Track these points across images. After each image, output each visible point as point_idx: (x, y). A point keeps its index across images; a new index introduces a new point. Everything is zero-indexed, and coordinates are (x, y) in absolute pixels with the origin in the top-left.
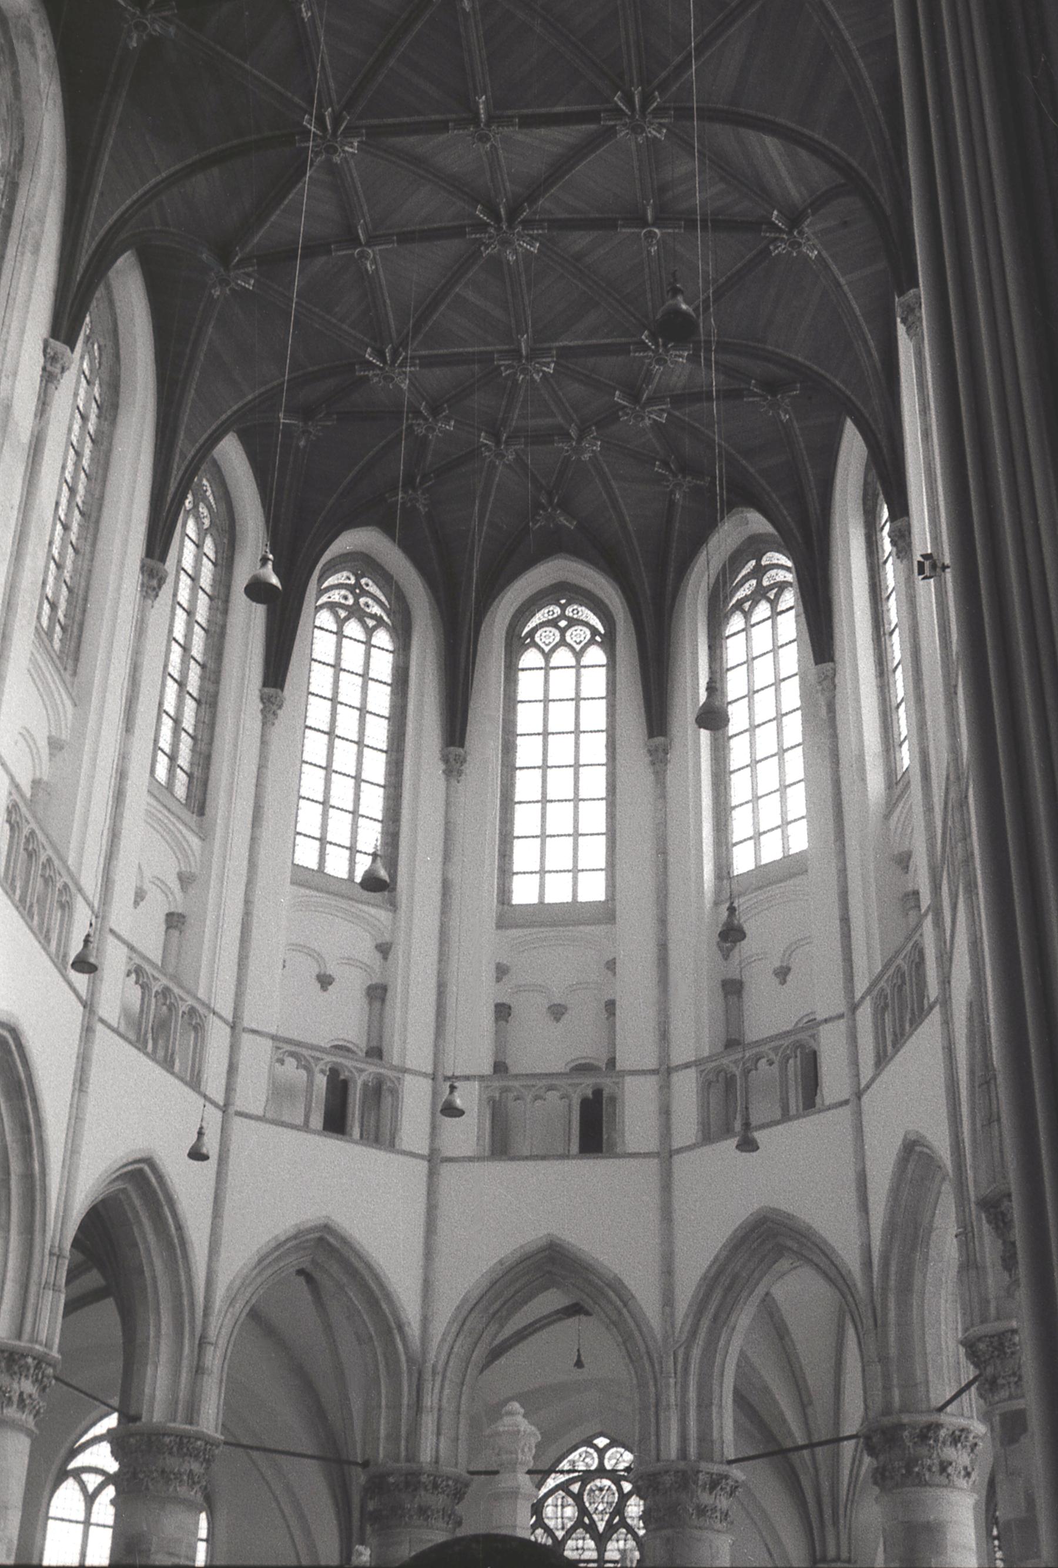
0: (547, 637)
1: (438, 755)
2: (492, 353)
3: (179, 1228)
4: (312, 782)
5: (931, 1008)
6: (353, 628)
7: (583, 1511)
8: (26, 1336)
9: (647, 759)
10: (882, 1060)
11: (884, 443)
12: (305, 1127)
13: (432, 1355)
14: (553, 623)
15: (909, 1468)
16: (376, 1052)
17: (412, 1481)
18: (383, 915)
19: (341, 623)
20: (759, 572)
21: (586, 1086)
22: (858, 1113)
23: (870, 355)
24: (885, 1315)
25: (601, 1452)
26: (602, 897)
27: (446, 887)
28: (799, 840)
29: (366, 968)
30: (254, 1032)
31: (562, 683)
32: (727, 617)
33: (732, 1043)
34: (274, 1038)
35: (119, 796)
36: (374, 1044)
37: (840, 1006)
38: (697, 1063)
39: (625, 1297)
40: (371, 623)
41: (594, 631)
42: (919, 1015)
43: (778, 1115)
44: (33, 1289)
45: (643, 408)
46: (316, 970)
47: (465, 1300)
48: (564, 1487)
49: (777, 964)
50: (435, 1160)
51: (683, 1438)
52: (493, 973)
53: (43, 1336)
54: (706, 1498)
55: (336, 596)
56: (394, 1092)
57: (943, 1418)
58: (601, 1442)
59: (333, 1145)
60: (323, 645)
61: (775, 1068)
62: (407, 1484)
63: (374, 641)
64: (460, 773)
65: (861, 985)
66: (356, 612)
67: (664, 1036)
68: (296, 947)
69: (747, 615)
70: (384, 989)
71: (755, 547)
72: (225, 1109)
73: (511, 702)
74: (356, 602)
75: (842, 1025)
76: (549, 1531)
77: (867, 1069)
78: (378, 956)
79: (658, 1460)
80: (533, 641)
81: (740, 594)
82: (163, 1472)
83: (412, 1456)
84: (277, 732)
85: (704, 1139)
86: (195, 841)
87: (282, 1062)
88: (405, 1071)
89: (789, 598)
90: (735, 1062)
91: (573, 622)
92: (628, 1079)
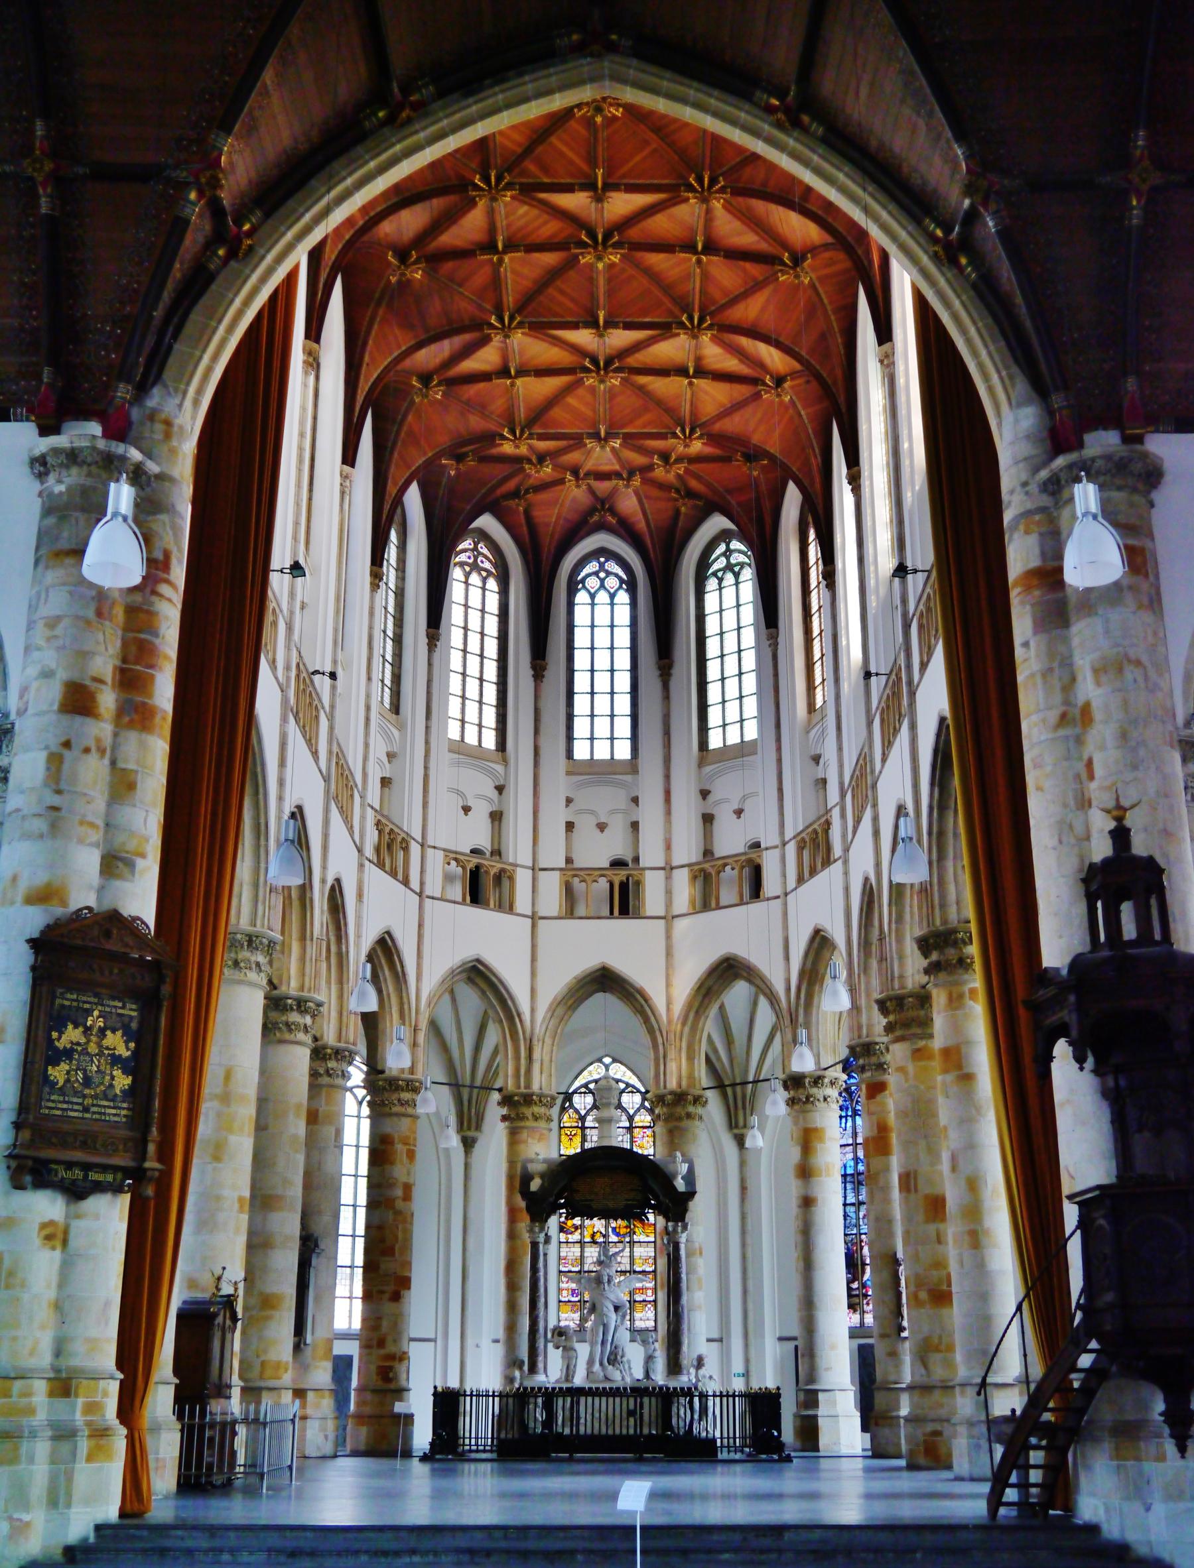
0: (593, 583)
1: (529, 665)
2: (582, 434)
3: (402, 966)
4: (455, 682)
5: (835, 861)
6: (475, 579)
8: (343, 1039)
9: (657, 673)
10: (801, 880)
11: (821, 512)
12: (463, 902)
13: (537, 1031)
14: (596, 574)
15: (808, 1098)
16: (497, 852)
17: (528, 1099)
18: (499, 768)
19: (467, 575)
20: (728, 553)
21: (619, 876)
22: (785, 904)
23: (815, 457)
24: (797, 1016)
25: (607, 1067)
26: (628, 757)
28: (752, 732)
29: (490, 801)
30: (434, 847)
32: (706, 578)
33: (708, 853)
34: (444, 850)
35: (367, 719)
36: (496, 847)
37: (776, 841)
38: (689, 865)
40: (484, 574)
42: (827, 862)
43: (736, 900)
44: (345, 1014)
45: (671, 465)
46: (461, 804)
47: (555, 999)
48: (586, 1086)
49: (736, 807)
50: (534, 918)
52: (564, 802)
53: (351, 1040)
54: (691, 1109)
55: (463, 557)
56: (511, 879)
57: (827, 1073)
60: (456, 591)
61: (736, 872)
62: (525, 1100)
63: (487, 586)
64: (543, 676)
65: (789, 834)
66: (475, 567)
67: (668, 847)
68: (451, 790)
70: (501, 814)
71: (724, 536)
72: (420, 895)
74: (476, 560)
75: (777, 852)
76: (577, 1111)
77: (792, 882)
78: (496, 792)
79: (665, 1087)
80: (584, 587)
81: (715, 567)
82: (399, 1100)
83: (528, 1086)
84: (436, 655)
86: (396, 732)
87: (449, 864)
88: (516, 865)
89: (748, 574)
90: (713, 867)
92: (647, 872)
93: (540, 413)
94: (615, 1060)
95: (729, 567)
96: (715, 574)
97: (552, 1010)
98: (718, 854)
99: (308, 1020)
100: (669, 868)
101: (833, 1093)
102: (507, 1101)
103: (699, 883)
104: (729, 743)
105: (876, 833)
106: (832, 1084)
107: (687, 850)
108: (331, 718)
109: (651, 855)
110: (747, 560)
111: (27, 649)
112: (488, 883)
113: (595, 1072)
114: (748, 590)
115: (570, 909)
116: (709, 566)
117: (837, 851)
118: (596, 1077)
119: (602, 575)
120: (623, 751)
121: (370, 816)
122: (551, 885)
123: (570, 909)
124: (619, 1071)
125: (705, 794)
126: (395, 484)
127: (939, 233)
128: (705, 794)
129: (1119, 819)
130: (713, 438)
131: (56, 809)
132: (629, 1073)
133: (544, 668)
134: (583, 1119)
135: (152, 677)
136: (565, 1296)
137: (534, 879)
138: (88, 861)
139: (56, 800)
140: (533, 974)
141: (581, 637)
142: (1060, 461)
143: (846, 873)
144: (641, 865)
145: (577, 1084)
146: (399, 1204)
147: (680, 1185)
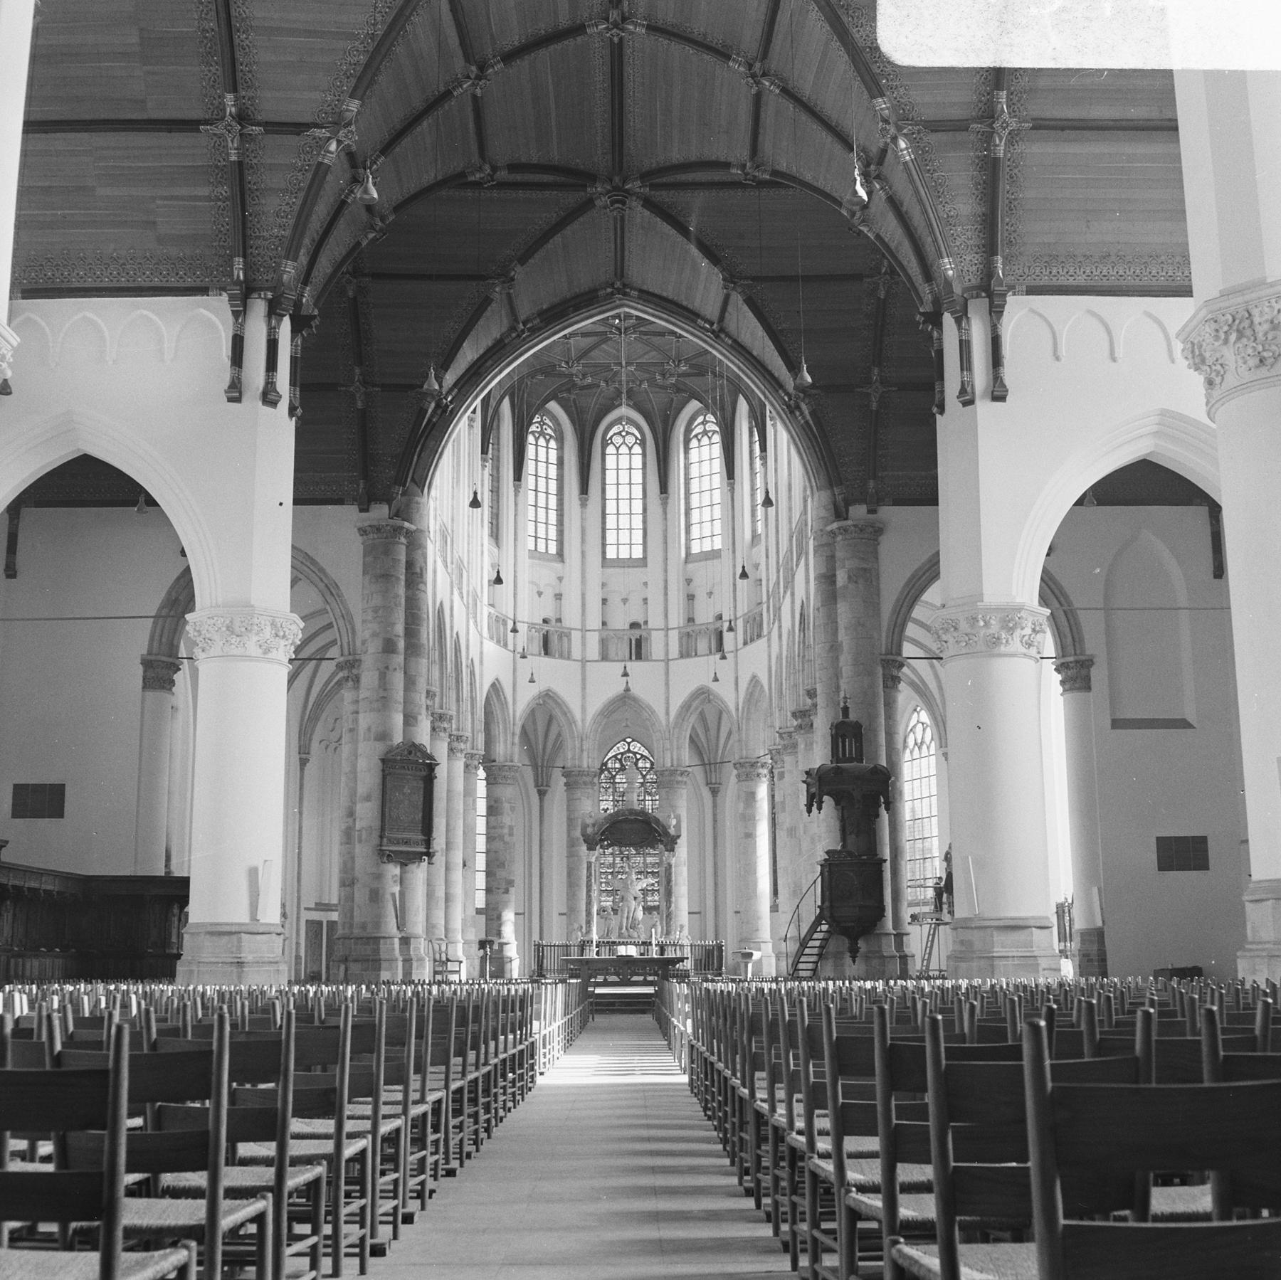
6: (542, 442)
7: (622, 765)
10: (745, 643)
12: (540, 654)
14: (619, 433)
16: (559, 620)
17: (581, 773)
18: (558, 566)
19: (537, 439)
20: (704, 423)
21: (636, 633)
22: (736, 657)
25: (629, 744)
27: (583, 554)
31: (624, 461)
32: (691, 440)
33: (691, 620)
38: (679, 628)
39: (653, 712)
41: (637, 438)
42: (759, 636)
46: (536, 590)
48: (615, 756)
50: (584, 662)
51: (672, 760)
54: (680, 778)
58: (629, 740)
59: (546, 660)
60: (530, 451)
65: (739, 614)
66: (542, 434)
67: (666, 616)
69: (699, 440)
70: (561, 595)
73: (604, 470)
85: (681, 652)
86: (496, 550)
89: (717, 438)
91: (628, 433)
92: (653, 632)
93: (585, 353)
94: (633, 741)
95: (705, 433)
96: (696, 436)
97: (594, 721)
98: (697, 622)
99: (462, 746)
100: (667, 629)
101: (765, 771)
102: (567, 774)
103: (684, 639)
104: (704, 550)
105: (780, 636)
106: (762, 766)
107: (676, 619)
108: (468, 572)
109: (655, 621)
110: (717, 429)
111: (364, 621)
112: (554, 640)
113: (622, 747)
114: (717, 450)
115: (605, 657)
116: (692, 430)
117: (765, 631)
118: (622, 751)
119: (624, 434)
120: (638, 553)
121: (486, 610)
122: (593, 641)
123: (605, 657)
124: (636, 747)
125: (689, 581)
126: (495, 398)
127: (786, 398)
128: (689, 581)
129: (845, 703)
130: (692, 366)
131: (383, 697)
132: (643, 748)
133: (587, 500)
134: (614, 777)
135: (419, 631)
136: (604, 887)
137: (583, 638)
138: (399, 719)
139: (382, 693)
140: (584, 697)
141: (611, 477)
142: (835, 525)
143: (769, 646)
144: (650, 626)
145: (610, 755)
146: (507, 838)
147: (672, 831)
